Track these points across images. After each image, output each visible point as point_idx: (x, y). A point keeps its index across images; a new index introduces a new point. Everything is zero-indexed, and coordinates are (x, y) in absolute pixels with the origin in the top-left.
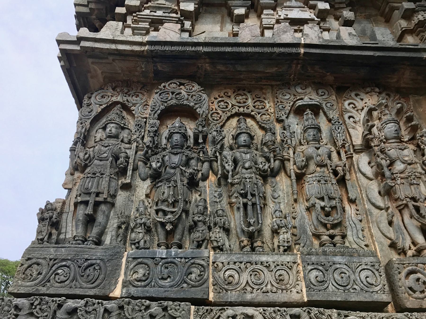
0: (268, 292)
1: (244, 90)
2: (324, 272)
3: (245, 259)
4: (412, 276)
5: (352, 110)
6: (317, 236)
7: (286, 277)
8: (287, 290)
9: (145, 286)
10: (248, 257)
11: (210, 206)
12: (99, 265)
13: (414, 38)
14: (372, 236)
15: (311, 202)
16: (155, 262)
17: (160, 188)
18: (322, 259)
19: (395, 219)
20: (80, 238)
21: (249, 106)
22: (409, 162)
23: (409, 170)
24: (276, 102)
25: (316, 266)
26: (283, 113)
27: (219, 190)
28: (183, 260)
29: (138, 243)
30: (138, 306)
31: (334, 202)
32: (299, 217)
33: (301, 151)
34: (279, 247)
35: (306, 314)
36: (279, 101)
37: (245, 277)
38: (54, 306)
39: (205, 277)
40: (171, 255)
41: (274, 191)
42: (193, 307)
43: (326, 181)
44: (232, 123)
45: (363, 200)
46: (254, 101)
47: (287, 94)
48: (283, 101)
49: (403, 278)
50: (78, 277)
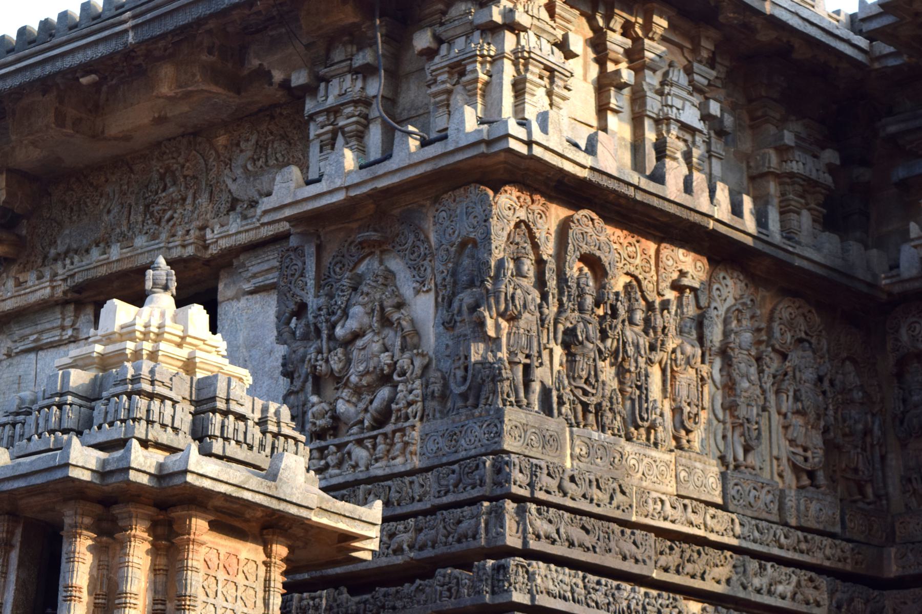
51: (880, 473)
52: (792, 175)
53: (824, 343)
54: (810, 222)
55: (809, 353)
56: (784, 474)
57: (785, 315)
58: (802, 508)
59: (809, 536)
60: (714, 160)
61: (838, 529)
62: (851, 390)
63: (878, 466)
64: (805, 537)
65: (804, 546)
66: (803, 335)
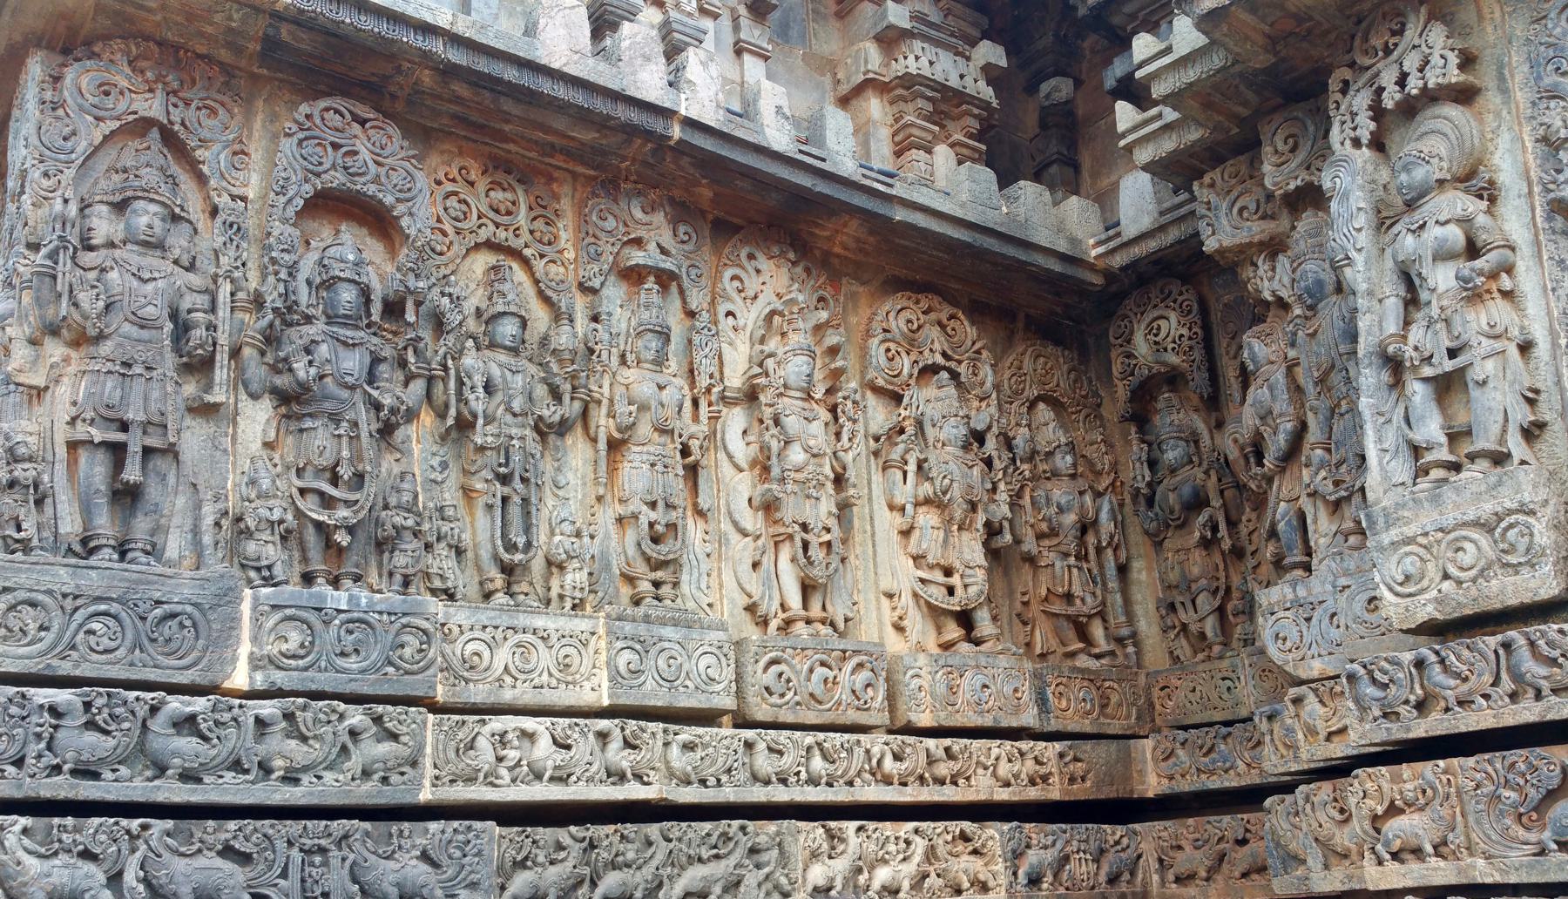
0: (542, 687)
1: (508, 172)
2: (643, 654)
3: (505, 620)
4: (775, 669)
5: (734, 295)
6: (631, 580)
7: (577, 660)
8: (574, 683)
9: (306, 669)
10: (511, 617)
11: (423, 489)
12: (190, 617)
13: (883, 107)
14: (721, 586)
15: (632, 507)
16: (325, 618)
17: (313, 433)
18: (642, 629)
19: (765, 560)
20: (112, 542)
21: (518, 229)
22: (815, 451)
23: (811, 468)
24: (583, 235)
25: (630, 643)
26: (597, 270)
27: (441, 453)
28: (385, 617)
29: (269, 567)
30: (325, 713)
31: (674, 514)
32: (601, 536)
33: (626, 382)
34: (561, 597)
35: (618, 730)
36: (591, 232)
37: (503, 656)
38: (142, 711)
39: (431, 655)
40: (359, 605)
41: (559, 469)
42: (431, 716)
43: (665, 467)
44: (474, 267)
45: (719, 513)
46: (533, 214)
47: (611, 218)
48: (598, 233)
49: (760, 671)
50: (146, 642)
51: (1118, 598)
52: (908, 81)
53: (987, 372)
54: (955, 162)
55: (951, 391)
56: (905, 623)
57: (898, 325)
58: (941, 689)
59: (957, 744)
60: (747, 57)
61: (1029, 718)
62: (1050, 454)
63: (1113, 584)
64: (947, 750)
65: (943, 769)
66: (939, 359)
